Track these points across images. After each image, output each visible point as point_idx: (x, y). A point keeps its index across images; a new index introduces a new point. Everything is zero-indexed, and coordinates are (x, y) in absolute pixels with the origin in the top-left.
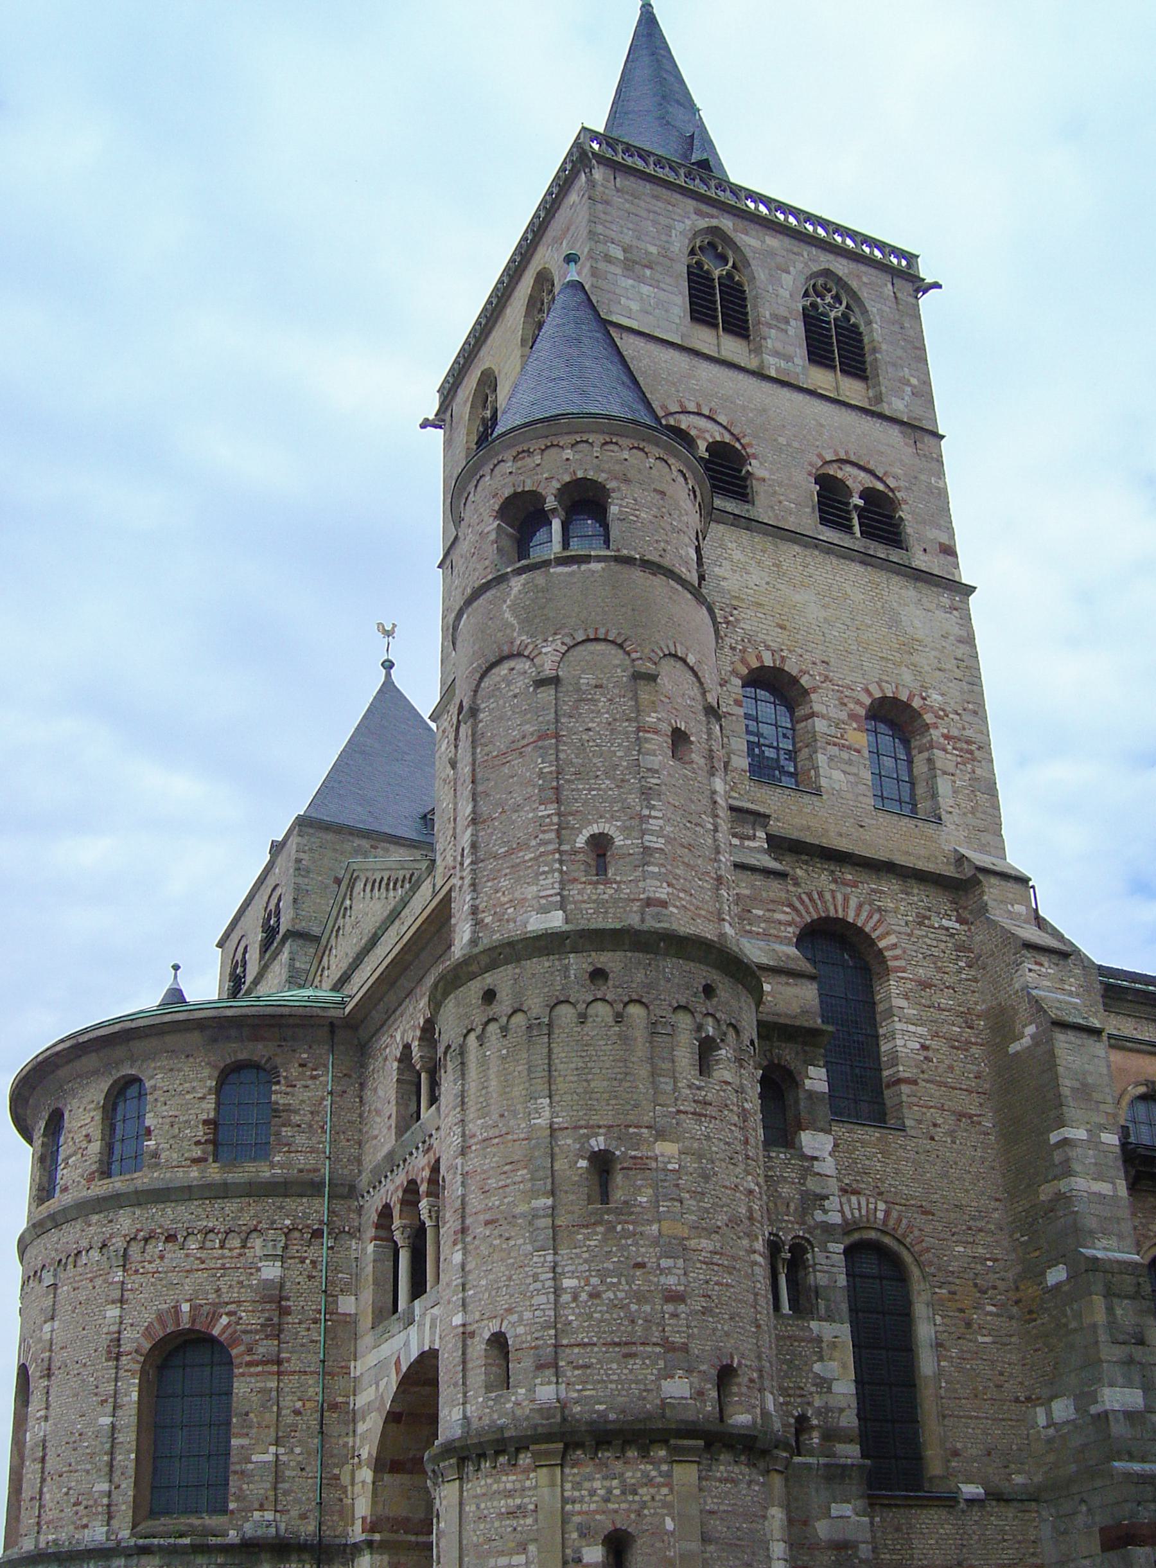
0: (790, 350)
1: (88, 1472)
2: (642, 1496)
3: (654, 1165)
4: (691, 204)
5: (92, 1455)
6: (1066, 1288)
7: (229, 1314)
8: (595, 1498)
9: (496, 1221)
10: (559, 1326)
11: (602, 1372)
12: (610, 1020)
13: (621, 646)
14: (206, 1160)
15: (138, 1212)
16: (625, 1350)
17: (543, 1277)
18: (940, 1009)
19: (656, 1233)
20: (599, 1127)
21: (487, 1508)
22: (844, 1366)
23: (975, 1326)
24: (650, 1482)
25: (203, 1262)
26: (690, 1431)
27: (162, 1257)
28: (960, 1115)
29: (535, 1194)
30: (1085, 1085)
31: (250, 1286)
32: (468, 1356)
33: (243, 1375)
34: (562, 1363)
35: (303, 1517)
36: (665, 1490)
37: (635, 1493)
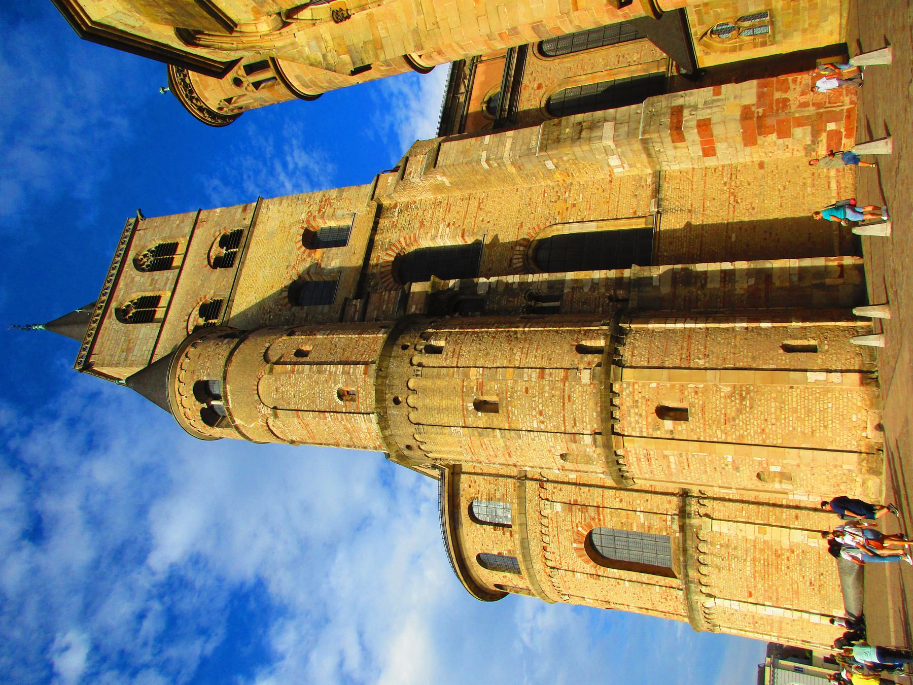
1: (651, 593)
3: (480, 380)
5: (643, 591)
6: (555, 161)
7: (577, 526)
8: (640, 421)
12: (416, 396)
14: (511, 531)
15: (534, 561)
17: (533, 437)
18: (432, 218)
19: (512, 381)
23: (575, 202)
27: (553, 553)
28: (479, 208)
29: (495, 436)
33: (604, 523)
35: (670, 502)
36: (636, 386)
37: (637, 401)
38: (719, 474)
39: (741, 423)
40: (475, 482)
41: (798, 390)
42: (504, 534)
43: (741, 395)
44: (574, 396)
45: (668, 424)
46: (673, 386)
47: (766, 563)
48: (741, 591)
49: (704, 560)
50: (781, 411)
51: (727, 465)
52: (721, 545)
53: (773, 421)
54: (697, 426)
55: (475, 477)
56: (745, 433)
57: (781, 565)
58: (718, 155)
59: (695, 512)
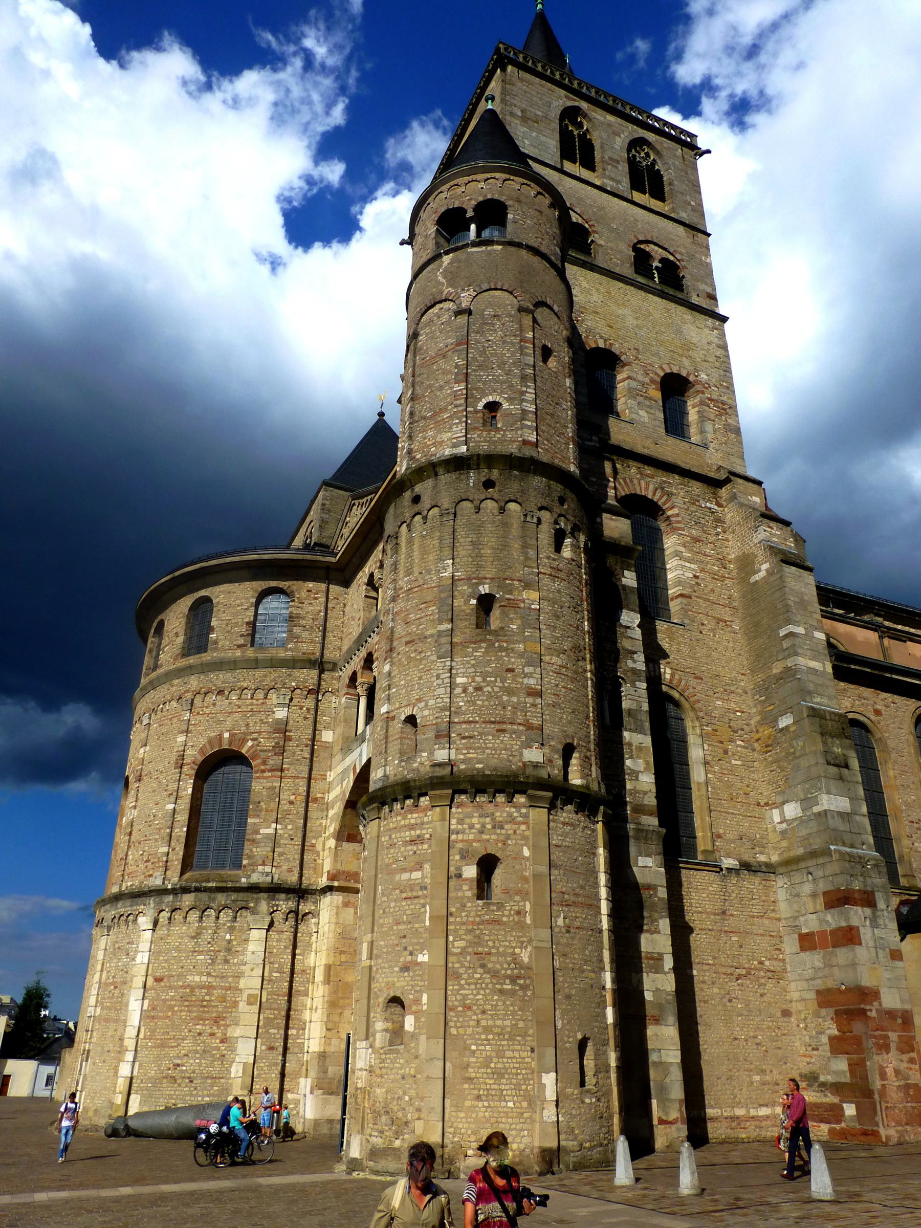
0: (619, 178)
1: (156, 840)
2: (507, 830)
3: (522, 605)
4: (563, 92)
5: (160, 829)
6: (792, 729)
7: (253, 740)
8: (473, 831)
9: (413, 641)
10: (453, 709)
11: (481, 741)
12: (496, 512)
13: (511, 293)
16: (498, 727)
18: (705, 554)
19: (522, 650)
20: (486, 578)
21: (396, 838)
22: (647, 763)
23: (730, 754)
24: (513, 820)
25: (239, 707)
26: (543, 784)
27: (214, 705)
28: (719, 620)
29: (441, 621)
30: (802, 600)
31: (267, 722)
32: (390, 733)
33: (259, 778)
34: (453, 735)
35: (290, 871)
36: (523, 827)
37: (502, 828)
38: (396, 942)
39: (478, 976)
40: (316, 598)
41: (529, 1060)
42: (242, 636)
43: (519, 977)
44: (505, 738)
45: (471, 872)
46: (525, 880)
47: (205, 1003)
48: (164, 968)
49: (208, 916)
50: (499, 1034)
51: (411, 954)
52: (230, 941)
53: (483, 1023)
54: (469, 912)
55: (323, 600)
56: (463, 982)
57: (202, 1025)
58: (802, 954)
59: (277, 906)
